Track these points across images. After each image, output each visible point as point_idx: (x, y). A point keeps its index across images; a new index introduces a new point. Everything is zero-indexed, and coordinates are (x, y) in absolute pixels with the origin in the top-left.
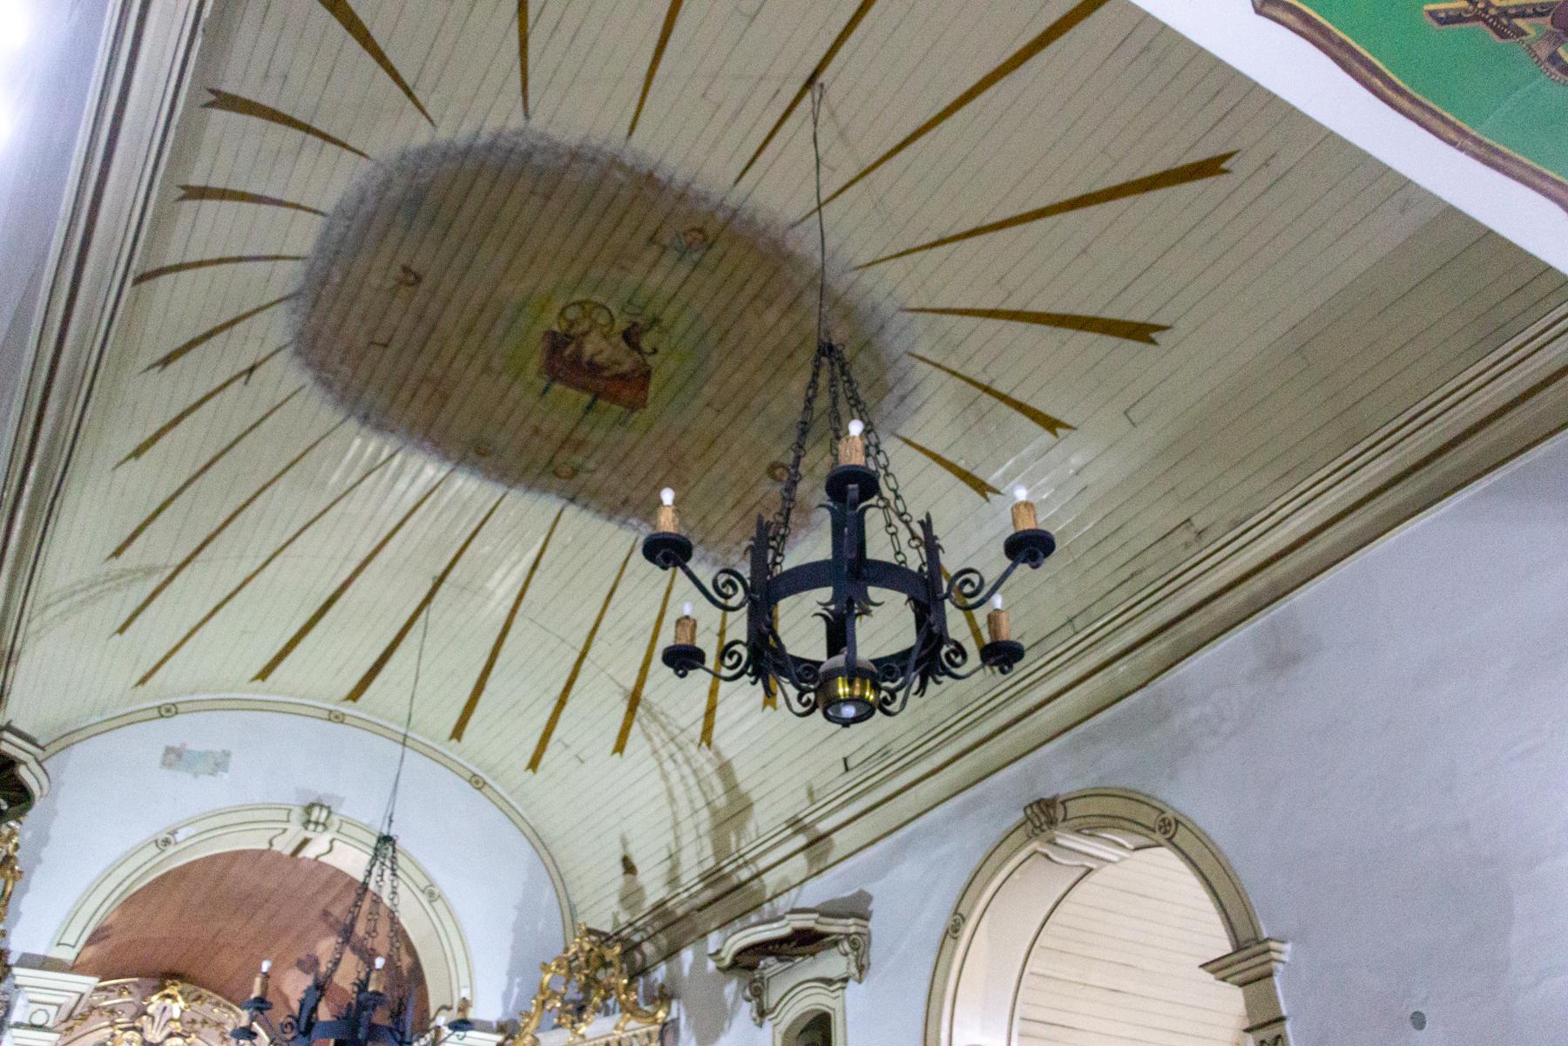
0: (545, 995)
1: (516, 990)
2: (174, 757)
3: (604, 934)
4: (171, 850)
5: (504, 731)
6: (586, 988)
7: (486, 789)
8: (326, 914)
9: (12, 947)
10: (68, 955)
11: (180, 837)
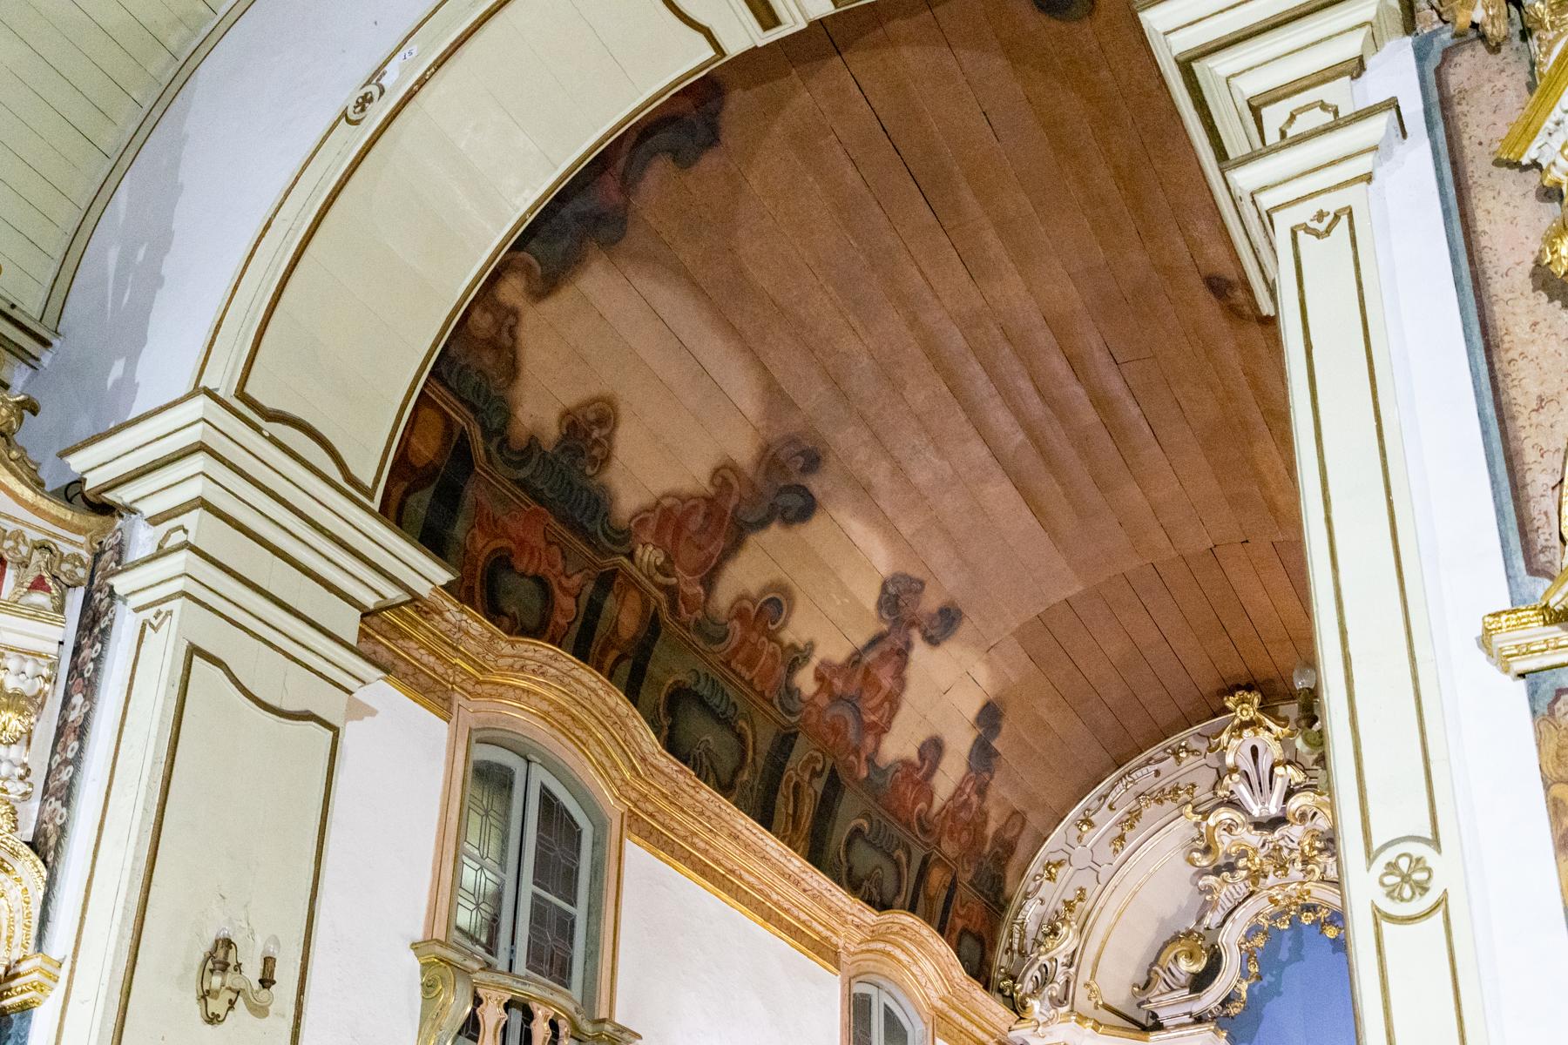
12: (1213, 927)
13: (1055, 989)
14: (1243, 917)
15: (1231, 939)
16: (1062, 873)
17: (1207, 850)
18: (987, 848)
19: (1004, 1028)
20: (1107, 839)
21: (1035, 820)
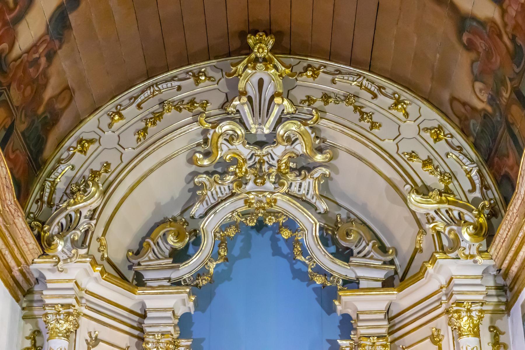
12: (197, 216)
13: (77, 235)
15: (210, 225)
16: (91, 148)
17: (207, 154)
18: (41, 109)
19: (30, 259)
20: (133, 129)
21: (80, 102)
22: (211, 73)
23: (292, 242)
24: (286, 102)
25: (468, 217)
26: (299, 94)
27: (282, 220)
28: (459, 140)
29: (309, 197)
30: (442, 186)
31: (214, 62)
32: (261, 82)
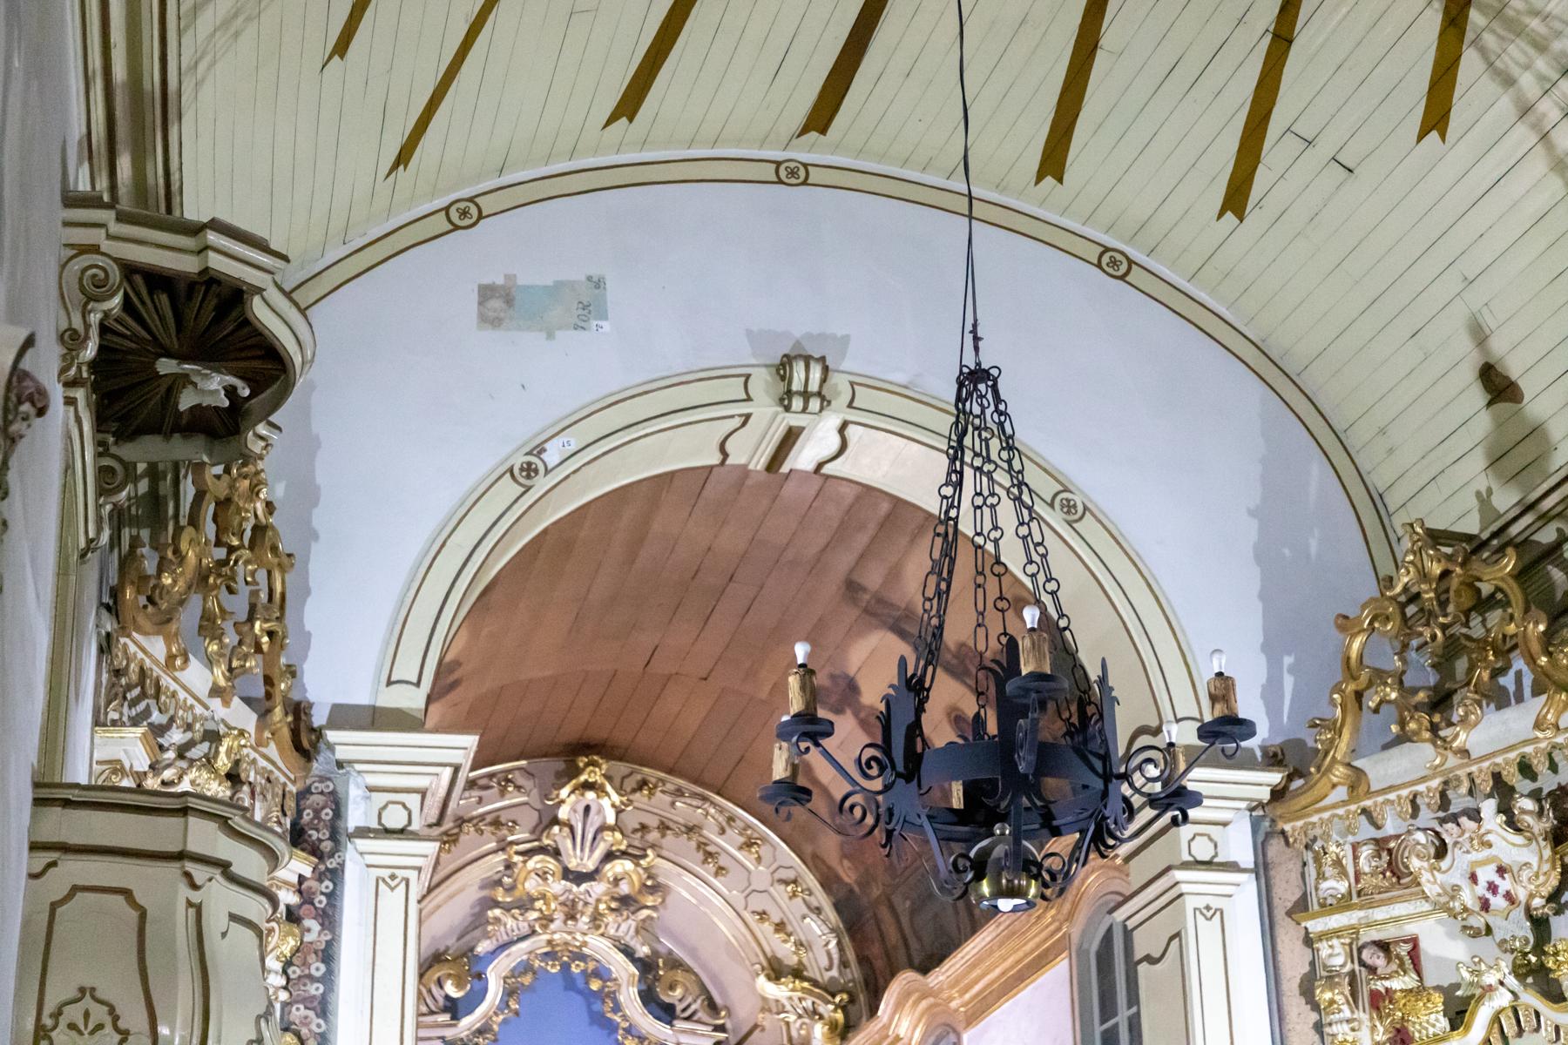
0: (1356, 684)
1: (1289, 682)
2: (499, 304)
3: (1469, 538)
4: (542, 484)
5: (1156, 141)
6: (1444, 663)
7: (1136, 276)
8: (852, 587)
9: (313, 694)
10: (413, 699)
11: (552, 456)
14: (519, 952)
22: (521, 780)
23: (601, 995)
24: (618, 835)
25: (822, 1008)
26: (631, 821)
27: (591, 966)
28: (821, 898)
29: (628, 938)
30: (795, 959)
31: (524, 762)
32: (587, 809)
